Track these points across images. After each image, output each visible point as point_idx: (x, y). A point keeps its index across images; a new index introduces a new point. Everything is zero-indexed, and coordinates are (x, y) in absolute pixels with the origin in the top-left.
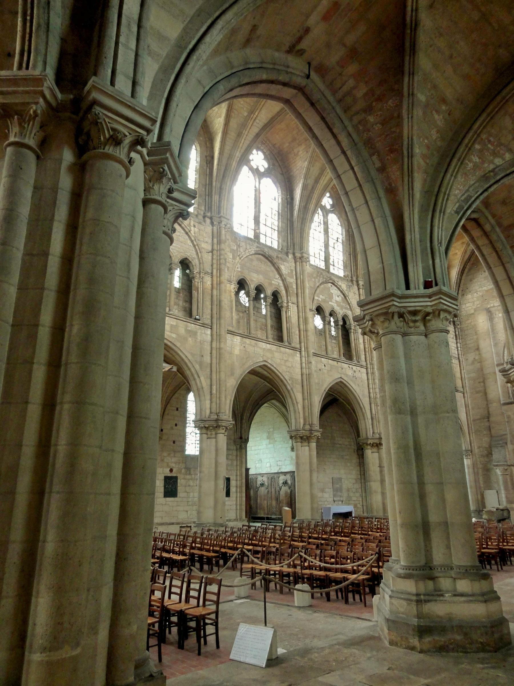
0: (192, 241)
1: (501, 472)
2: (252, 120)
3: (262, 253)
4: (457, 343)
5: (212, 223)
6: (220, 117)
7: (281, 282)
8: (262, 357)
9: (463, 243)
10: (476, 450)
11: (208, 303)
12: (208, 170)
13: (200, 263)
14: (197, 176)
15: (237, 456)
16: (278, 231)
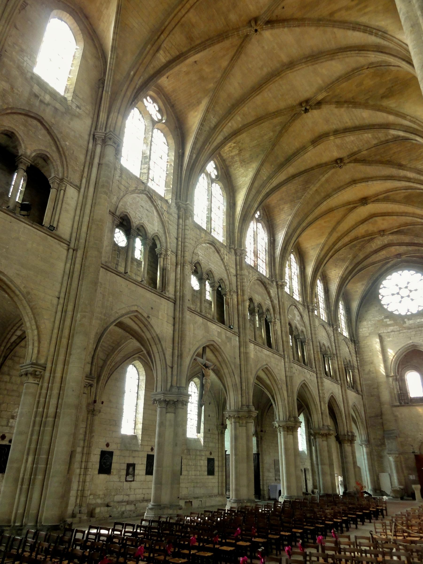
0: (225, 266)
1: (394, 459)
3: (260, 279)
4: (357, 357)
5: (236, 254)
6: (246, 176)
7: (270, 302)
9: (363, 284)
10: (372, 441)
11: (236, 316)
12: (231, 213)
13: (230, 284)
15: (218, 439)
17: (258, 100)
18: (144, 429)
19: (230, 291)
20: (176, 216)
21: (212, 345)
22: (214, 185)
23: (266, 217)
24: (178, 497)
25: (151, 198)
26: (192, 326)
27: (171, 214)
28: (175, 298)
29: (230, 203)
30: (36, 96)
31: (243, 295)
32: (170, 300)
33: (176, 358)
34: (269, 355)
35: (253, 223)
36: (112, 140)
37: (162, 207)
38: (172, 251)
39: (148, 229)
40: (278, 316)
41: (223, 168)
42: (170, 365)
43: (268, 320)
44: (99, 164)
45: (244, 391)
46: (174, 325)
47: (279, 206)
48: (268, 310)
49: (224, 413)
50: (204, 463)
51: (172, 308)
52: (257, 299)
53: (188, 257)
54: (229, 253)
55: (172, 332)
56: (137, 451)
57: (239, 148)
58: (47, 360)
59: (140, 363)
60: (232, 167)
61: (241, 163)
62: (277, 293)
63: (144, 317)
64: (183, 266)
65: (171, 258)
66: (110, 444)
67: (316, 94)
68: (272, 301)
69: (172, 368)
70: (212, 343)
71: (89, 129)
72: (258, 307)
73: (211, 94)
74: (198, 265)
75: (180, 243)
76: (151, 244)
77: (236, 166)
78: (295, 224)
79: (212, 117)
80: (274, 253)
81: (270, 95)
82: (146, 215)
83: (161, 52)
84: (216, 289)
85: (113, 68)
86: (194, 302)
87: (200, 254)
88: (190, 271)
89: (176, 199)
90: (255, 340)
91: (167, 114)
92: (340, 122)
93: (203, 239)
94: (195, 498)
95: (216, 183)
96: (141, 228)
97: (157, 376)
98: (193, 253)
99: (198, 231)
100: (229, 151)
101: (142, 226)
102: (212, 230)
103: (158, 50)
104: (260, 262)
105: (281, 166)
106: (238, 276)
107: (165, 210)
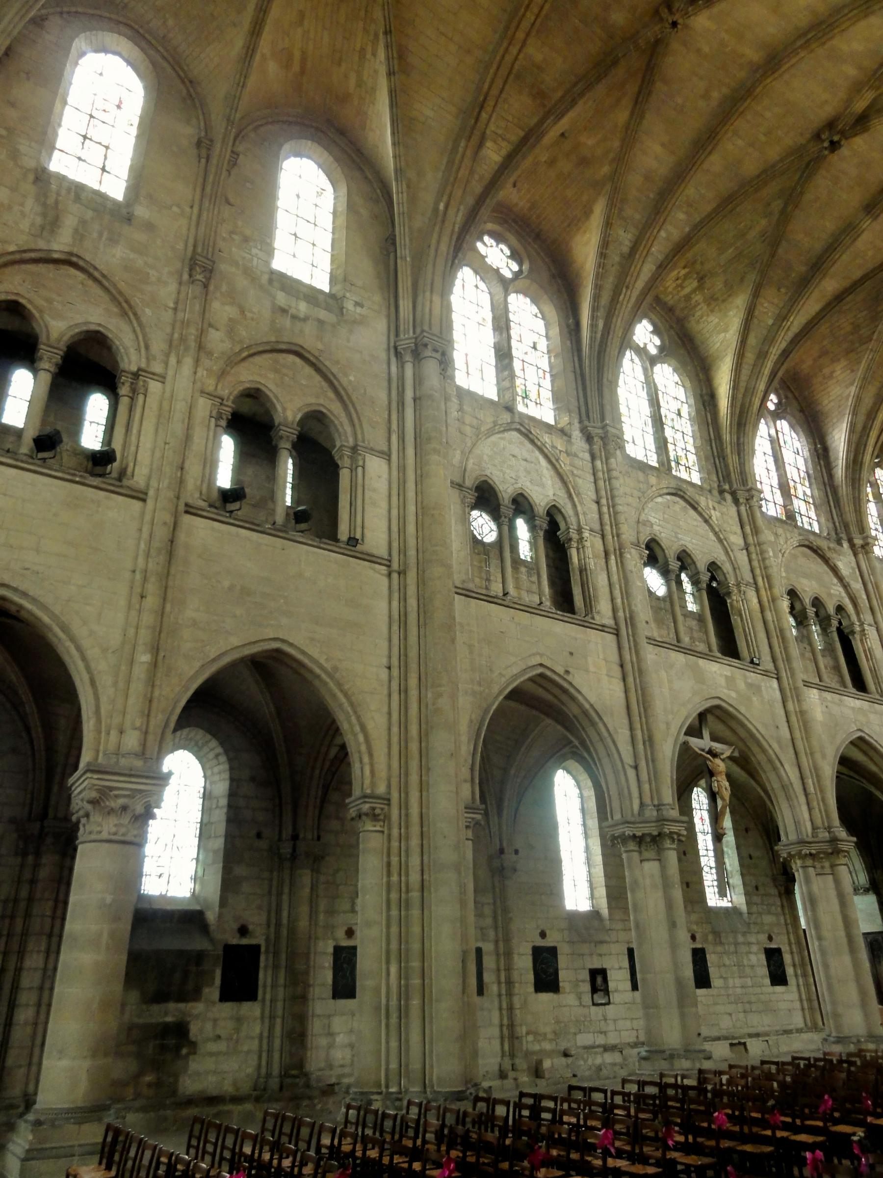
0: (716, 534)
3: (807, 543)
5: (736, 501)
6: (726, 330)
7: (841, 590)
8: (855, 723)
11: (762, 635)
13: (734, 569)
14: (696, 428)
16: (814, 504)
17: (715, 162)
18: (609, 896)
19: (738, 585)
20: (587, 456)
21: (718, 707)
22: (658, 368)
23: (795, 404)
24: (699, 1034)
25: (528, 435)
26: (663, 674)
27: (576, 455)
28: (616, 624)
29: (701, 396)
30: (284, 311)
31: (771, 587)
32: (606, 629)
33: (641, 747)
34: (860, 709)
35: (766, 424)
36: (429, 347)
37: (553, 447)
38: (591, 530)
39: (534, 497)
40: (868, 617)
42: (631, 762)
43: (846, 631)
44: (415, 400)
45: (812, 797)
46: (624, 679)
47: (821, 370)
48: (840, 609)
49: (776, 848)
50: (759, 960)
51: (614, 645)
52: (808, 589)
53: (628, 534)
54: (719, 503)
55: (622, 695)
56: (606, 942)
57: (697, 273)
58: (389, 786)
59: (577, 764)
61: (709, 305)
62: (855, 566)
63: (559, 675)
64: (621, 555)
65: (593, 545)
66: (548, 932)
67: (849, 102)
68: (846, 586)
69: (636, 767)
70: (717, 702)
71: (385, 339)
72: (813, 605)
73: (608, 187)
74: (653, 545)
75: (605, 509)
76: (545, 526)
77: (698, 314)
79: (621, 232)
80: (831, 476)
82: (526, 470)
83: (489, 144)
84: (705, 585)
85: (406, 210)
86: (660, 622)
87: (653, 520)
88: (638, 561)
89: (581, 422)
90: (820, 681)
91: (529, 257)
93: (654, 489)
94: (751, 1036)
95: (661, 363)
96: (520, 499)
97: (608, 788)
98: (638, 522)
99: (641, 476)
100: (677, 286)
101: (522, 495)
102: (673, 464)
103: (481, 145)
104: (799, 505)
105: (803, 285)
106: (752, 549)
107: (561, 451)
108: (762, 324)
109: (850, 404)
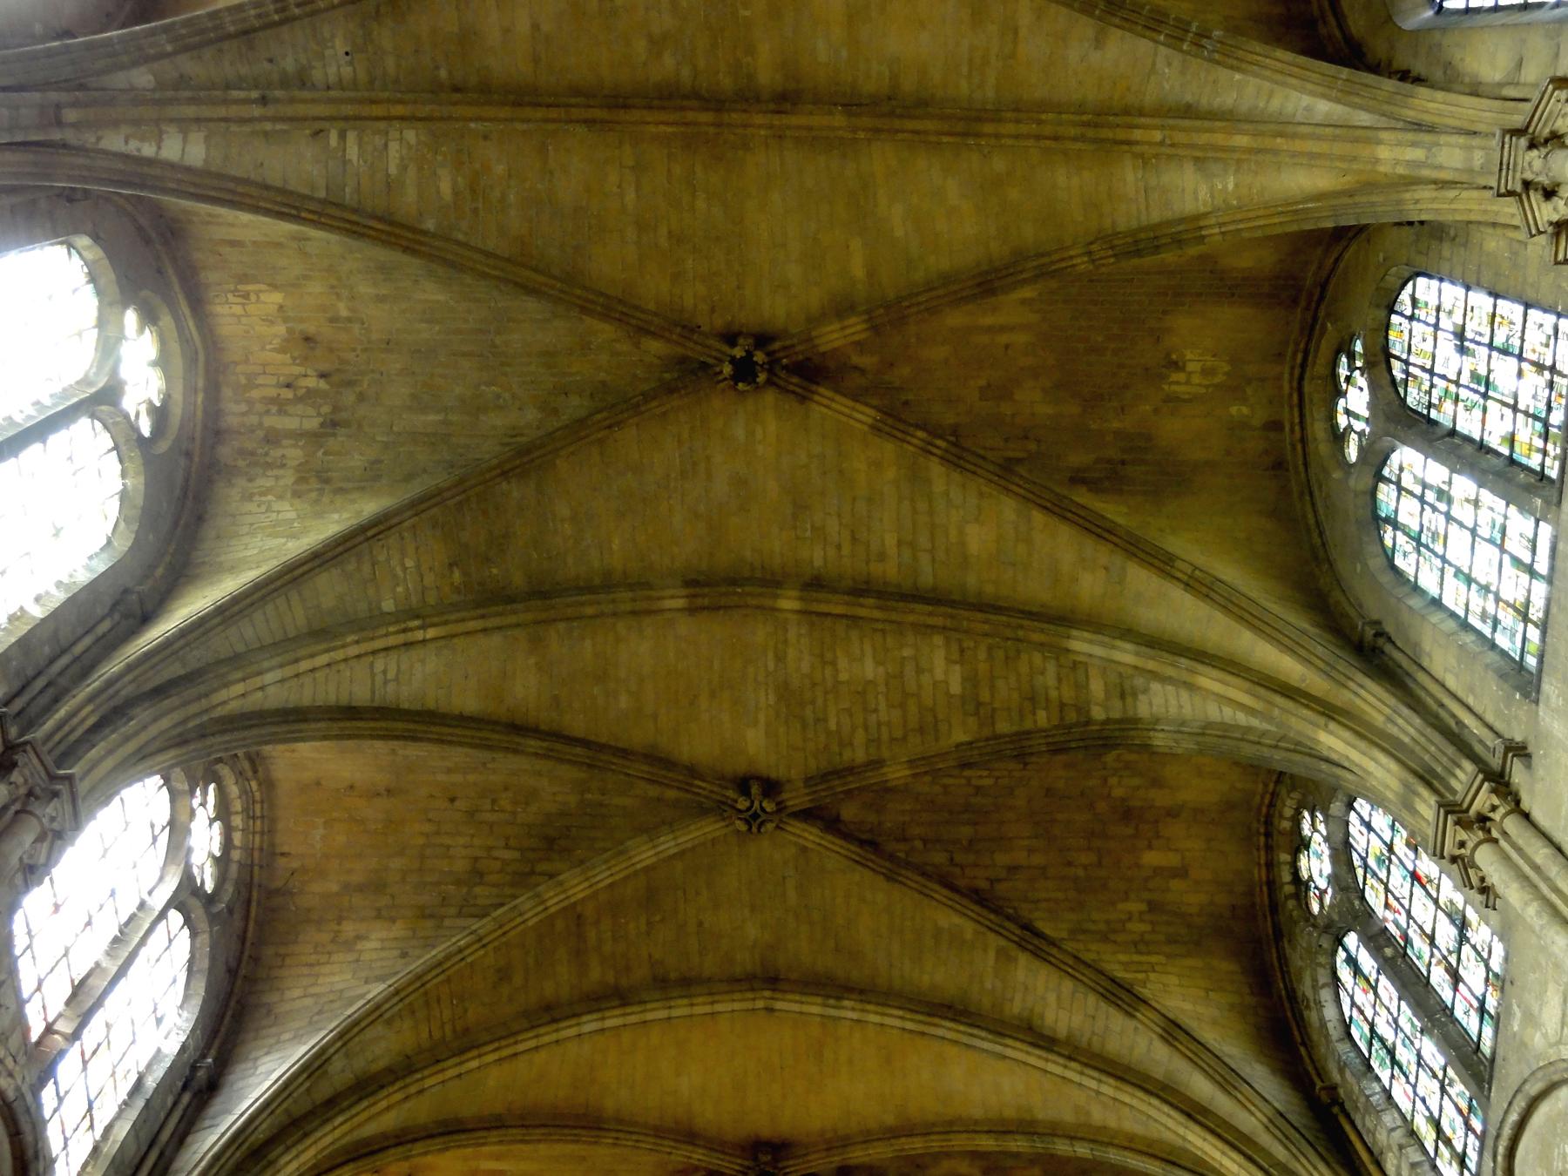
2: (401, 638)
41: (188, 455)
47: (340, 920)
60: (241, 482)
61: (302, 480)
67: (815, 320)
78: (382, 1047)
79: (340, 46)
80: (182, 1137)
81: (630, 196)
92: (854, 540)
108: (371, 591)
109: (349, 1012)
